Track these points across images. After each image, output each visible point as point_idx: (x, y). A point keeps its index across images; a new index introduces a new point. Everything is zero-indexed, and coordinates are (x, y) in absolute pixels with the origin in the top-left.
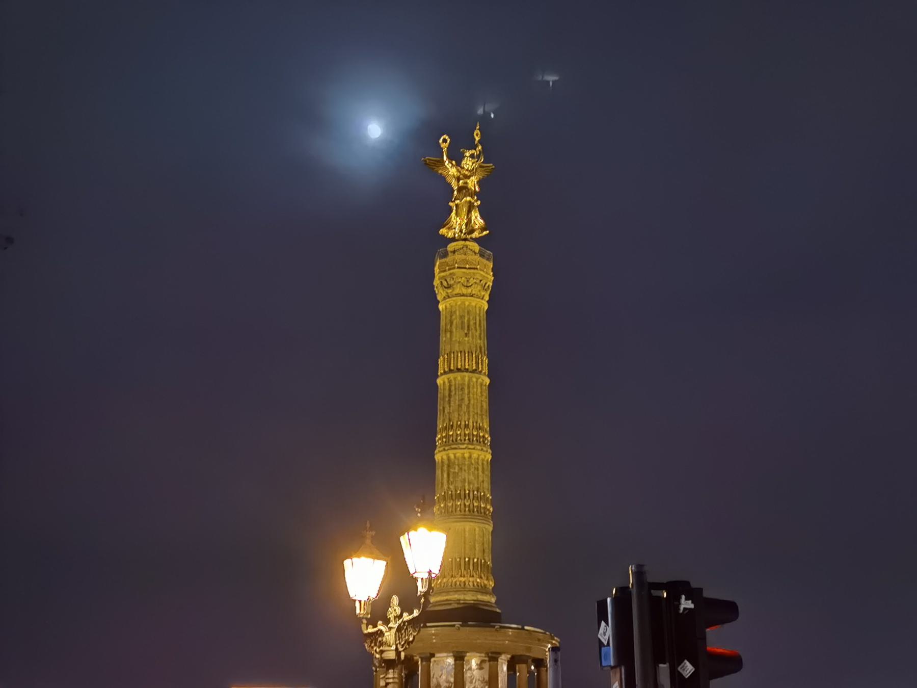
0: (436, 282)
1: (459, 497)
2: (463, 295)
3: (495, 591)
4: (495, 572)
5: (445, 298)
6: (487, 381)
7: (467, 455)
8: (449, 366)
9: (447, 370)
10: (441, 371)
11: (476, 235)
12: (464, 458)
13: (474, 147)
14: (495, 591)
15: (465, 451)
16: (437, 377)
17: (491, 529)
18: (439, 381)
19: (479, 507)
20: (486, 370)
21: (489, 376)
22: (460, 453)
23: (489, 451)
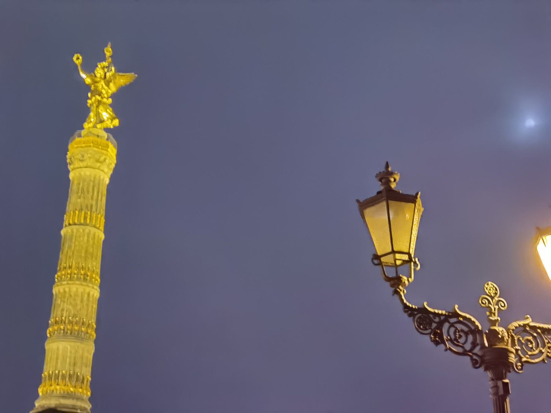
1: (77, 323)
2: (81, 168)
4: (93, 385)
6: (102, 236)
7: (67, 290)
8: (73, 220)
9: (71, 222)
10: (66, 223)
11: (104, 125)
12: (65, 291)
13: (104, 59)
14: (91, 400)
15: (65, 286)
16: (61, 228)
18: (62, 232)
19: (79, 331)
20: (102, 228)
21: (105, 232)
22: (77, 288)
23: (99, 290)
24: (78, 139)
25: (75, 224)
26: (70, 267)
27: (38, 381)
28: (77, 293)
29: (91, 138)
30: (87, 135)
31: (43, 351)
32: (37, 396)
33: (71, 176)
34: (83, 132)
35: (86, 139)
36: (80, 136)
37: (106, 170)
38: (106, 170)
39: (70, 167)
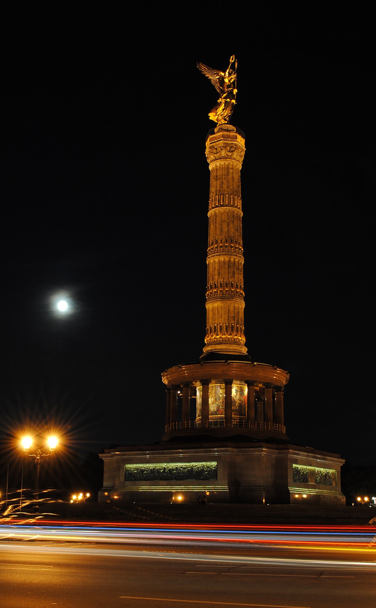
0: (207, 151)
3: (246, 345)
5: (212, 161)
14: (246, 345)
17: (242, 305)
18: (209, 214)
24: (211, 137)
25: (216, 207)
26: (217, 242)
27: (204, 333)
28: (223, 261)
29: (221, 133)
30: (218, 132)
31: (204, 310)
32: (204, 345)
33: (210, 168)
34: (216, 130)
35: (218, 134)
36: (214, 133)
37: (238, 158)
38: (238, 158)
39: (209, 161)
